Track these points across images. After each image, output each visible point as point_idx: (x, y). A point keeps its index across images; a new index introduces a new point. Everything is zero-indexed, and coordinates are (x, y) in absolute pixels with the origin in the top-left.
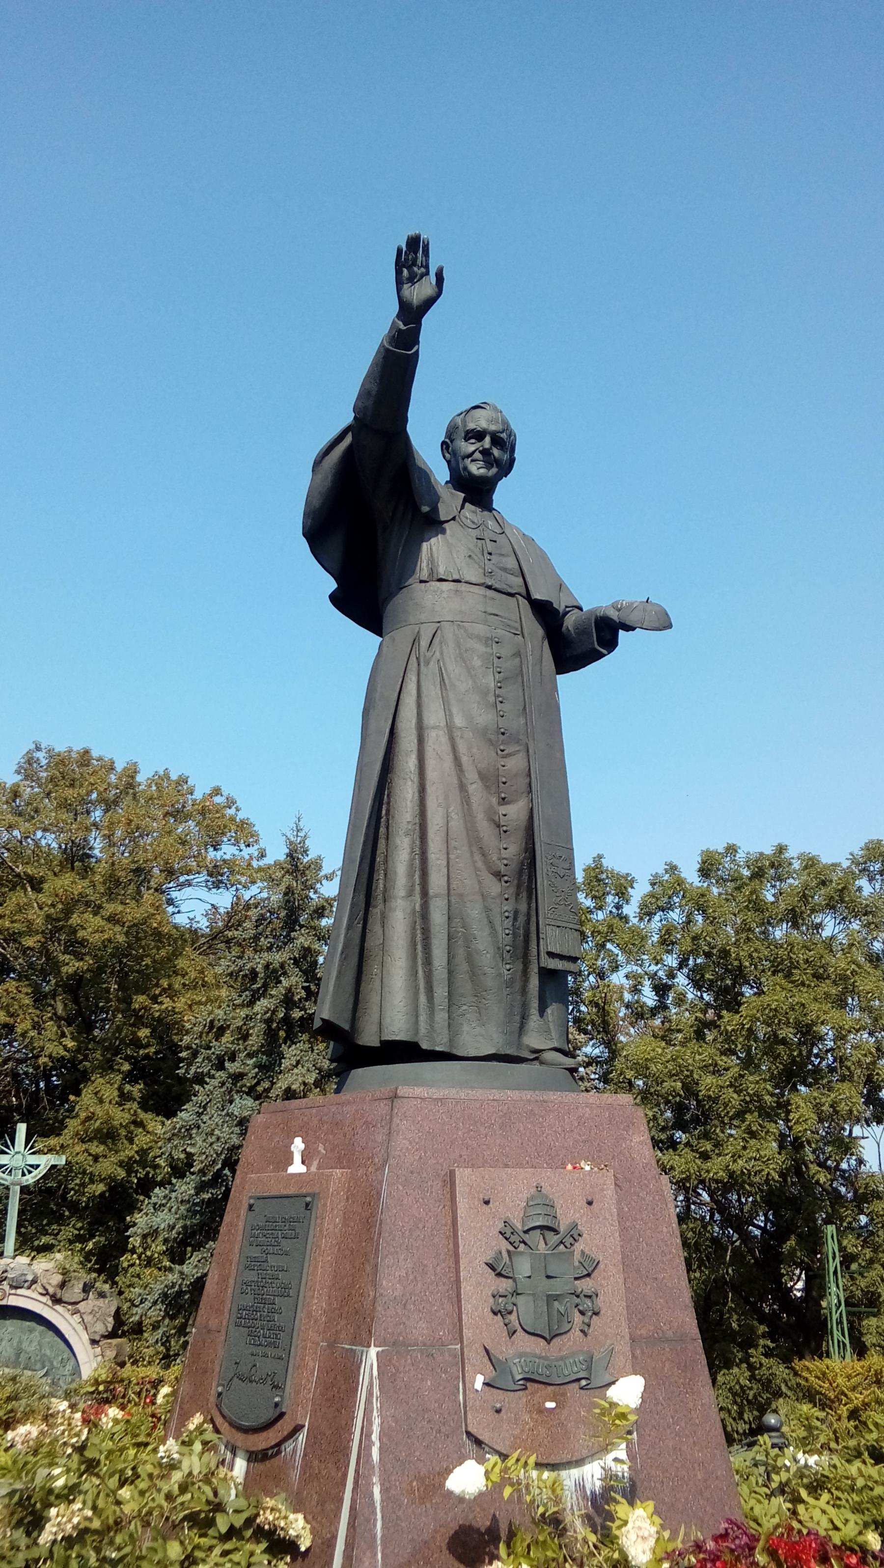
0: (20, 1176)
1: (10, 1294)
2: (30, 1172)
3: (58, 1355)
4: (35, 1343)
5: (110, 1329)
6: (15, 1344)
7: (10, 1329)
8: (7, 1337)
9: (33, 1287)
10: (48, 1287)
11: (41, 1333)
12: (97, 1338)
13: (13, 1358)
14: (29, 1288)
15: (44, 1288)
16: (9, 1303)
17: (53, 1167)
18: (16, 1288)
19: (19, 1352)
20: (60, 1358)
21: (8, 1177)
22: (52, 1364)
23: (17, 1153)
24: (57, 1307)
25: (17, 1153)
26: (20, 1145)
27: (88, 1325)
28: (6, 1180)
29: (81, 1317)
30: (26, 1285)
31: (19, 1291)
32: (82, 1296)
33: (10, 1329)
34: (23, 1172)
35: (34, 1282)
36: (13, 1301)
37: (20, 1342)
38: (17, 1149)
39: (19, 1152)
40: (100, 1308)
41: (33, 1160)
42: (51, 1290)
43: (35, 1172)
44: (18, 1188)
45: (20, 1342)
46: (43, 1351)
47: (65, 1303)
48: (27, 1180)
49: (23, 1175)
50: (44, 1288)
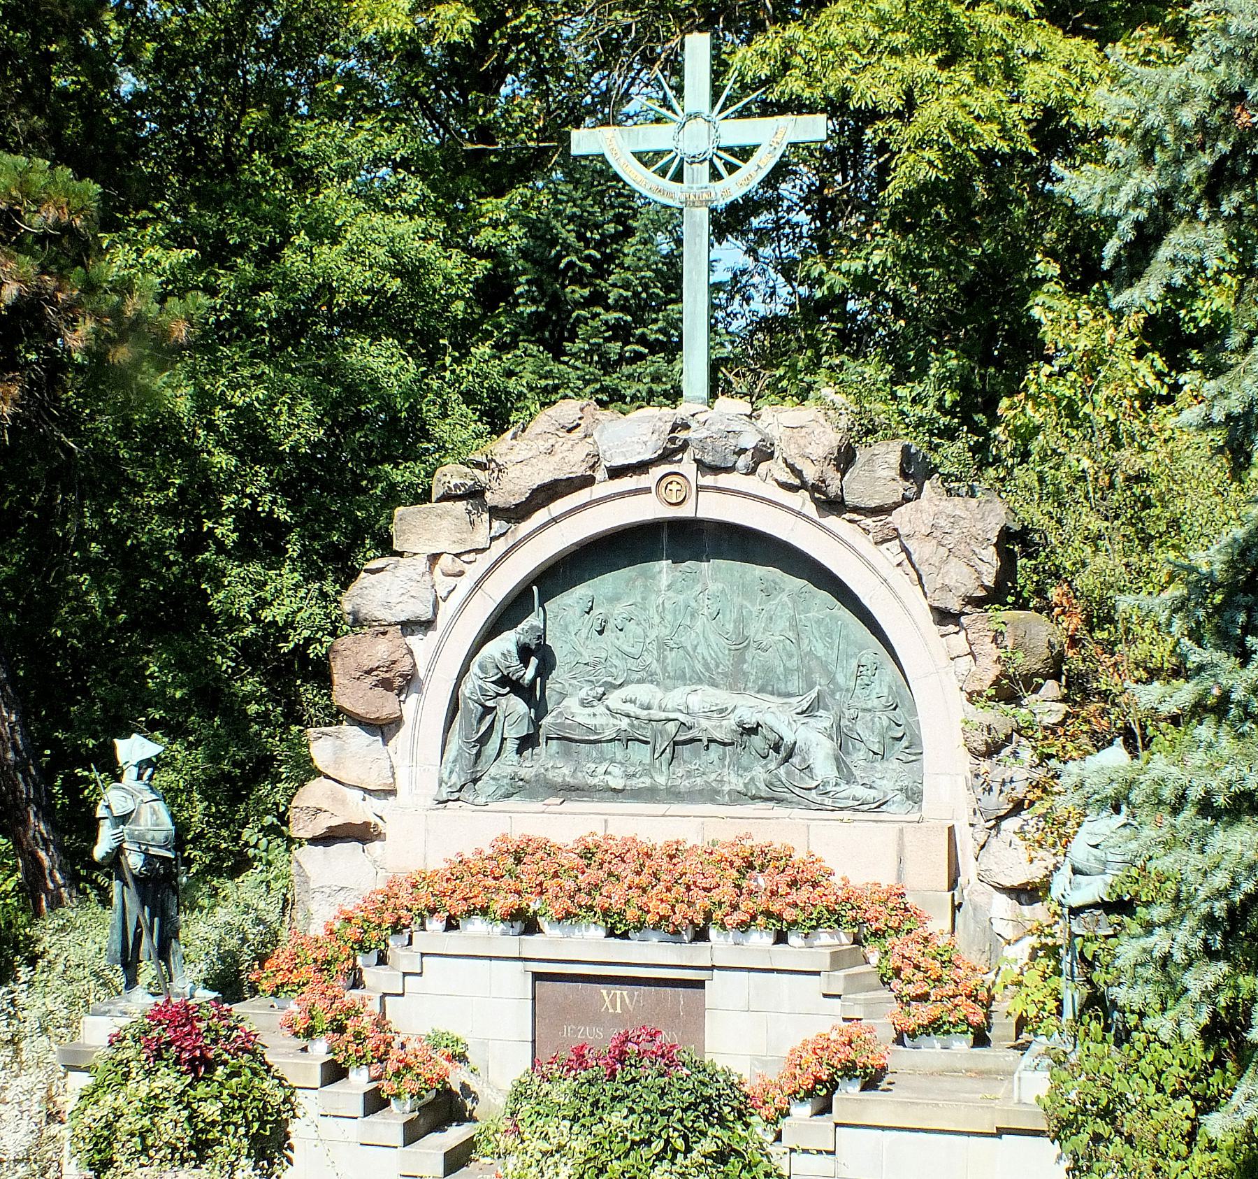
2: (732, 169)
3: (848, 657)
4: (782, 624)
5: (989, 581)
6: (730, 627)
7: (713, 587)
8: (706, 608)
9: (763, 468)
11: (796, 596)
12: (955, 605)
13: (727, 663)
14: (752, 471)
15: (792, 468)
18: (716, 470)
19: (741, 645)
20: (854, 663)
22: (832, 680)
24: (832, 521)
25: (696, 115)
27: (924, 570)
28: (669, 194)
29: (905, 549)
30: (743, 461)
31: (723, 480)
32: (900, 487)
33: (713, 587)
35: (763, 454)
36: (713, 508)
37: (741, 621)
39: (696, 115)
40: (955, 519)
41: (738, 132)
42: (811, 474)
43: (746, 169)
44: (703, 215)
45: (741, 621)
46: (805, 646)
47: (856, 510)
48: (726, 192)
50: (792, 468)
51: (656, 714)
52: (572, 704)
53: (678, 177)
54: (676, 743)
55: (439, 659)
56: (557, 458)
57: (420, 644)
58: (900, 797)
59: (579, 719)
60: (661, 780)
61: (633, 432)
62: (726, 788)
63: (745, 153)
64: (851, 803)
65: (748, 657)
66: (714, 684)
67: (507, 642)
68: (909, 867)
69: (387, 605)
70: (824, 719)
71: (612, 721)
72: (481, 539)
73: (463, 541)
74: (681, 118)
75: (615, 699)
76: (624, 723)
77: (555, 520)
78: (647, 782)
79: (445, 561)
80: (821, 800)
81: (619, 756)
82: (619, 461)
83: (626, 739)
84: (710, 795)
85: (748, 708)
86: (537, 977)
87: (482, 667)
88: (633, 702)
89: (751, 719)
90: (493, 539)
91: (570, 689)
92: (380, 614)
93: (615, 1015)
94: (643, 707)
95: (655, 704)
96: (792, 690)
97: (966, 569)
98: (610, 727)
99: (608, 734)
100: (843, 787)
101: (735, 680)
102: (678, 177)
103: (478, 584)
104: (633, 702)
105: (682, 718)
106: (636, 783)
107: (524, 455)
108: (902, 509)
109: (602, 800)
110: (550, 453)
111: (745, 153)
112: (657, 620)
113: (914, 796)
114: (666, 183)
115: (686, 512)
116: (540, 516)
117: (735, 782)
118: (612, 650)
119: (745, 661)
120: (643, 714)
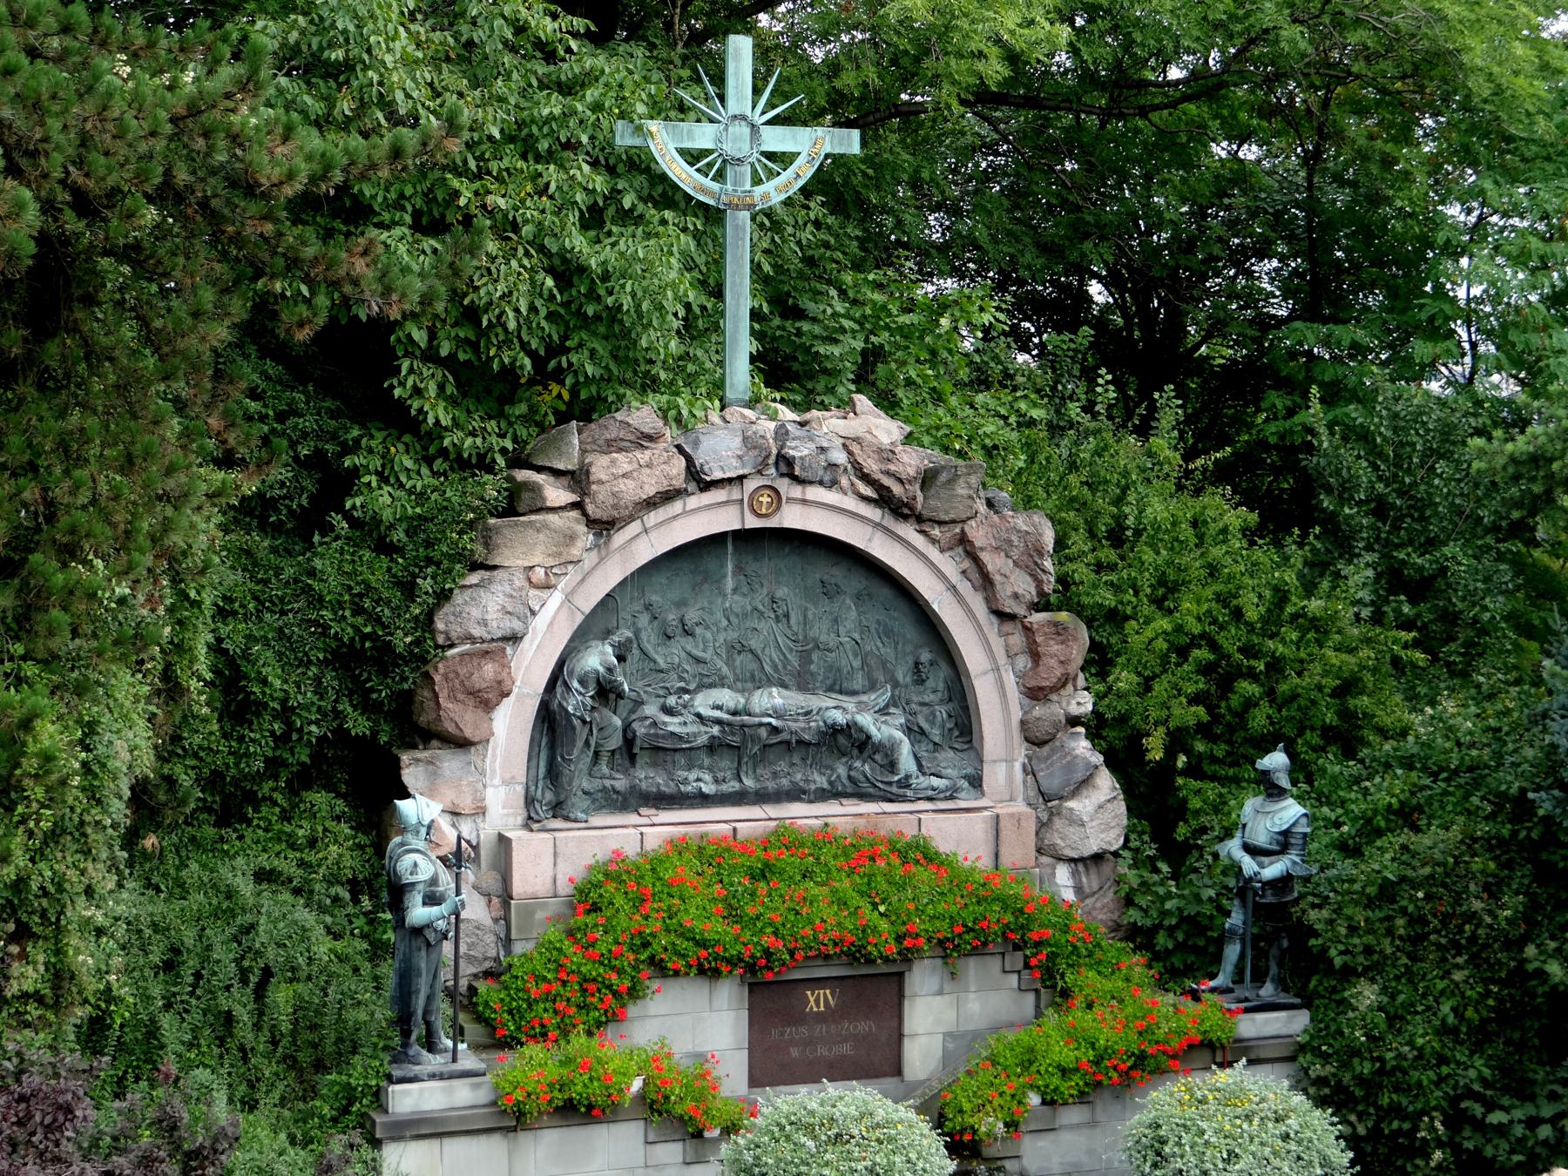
0: (748, 187)
2: (771, 174)
10: (887, 481)
16: (786, 525)
21: (715, 186)
23: (735, 117)
26: (740, 99)
34: (754, 171)
36: (792, 518)
41: (778, 139)
43: (785, 176)
48: (765, 196)
49: (757, 181)
52: (651, 709)
53: (720, 176)
58: (966, 784)
59: (670, 728)
60: (749, 782)
62: (813, 787)
64: (930, 793)
65: (815, 657)
66: (785, 687)
68: (1003, 850)
69: (484, 623)
71: (703, 729)
72: (575, 552)
73: (560, 554)
74: (722, 116)
76: (716, 730)
80: (897, 792)
81: (707, 761)
82: (718, 475)
83: (713, 747)
85: (837, 709)
87: (581, 682)
88: (719, 708)
89: (839, 718)
91: (644, 696)
92: (477, 632)
93: (818, 1013)
94: (728, 712)
96: (857, 685)
97: (1029, 579)
98: (704, 734)
99: (702, 740)
100: (922, 779)
101: (804, 683)
102: (720, 176)
103: (568, 598)
104: (719, 708)
105: (773, 722)
107: (627, 467)
108: (973, 523)
109: (692, 806)
110: (649, 466)
111: (784, 159)
112: (725, 623)
113: (976, 782)
114: (707, 182)
116: (635, 527)
117: (821, 781)
118: (683, 655)
119: (811, 662)
120: (725, 716)
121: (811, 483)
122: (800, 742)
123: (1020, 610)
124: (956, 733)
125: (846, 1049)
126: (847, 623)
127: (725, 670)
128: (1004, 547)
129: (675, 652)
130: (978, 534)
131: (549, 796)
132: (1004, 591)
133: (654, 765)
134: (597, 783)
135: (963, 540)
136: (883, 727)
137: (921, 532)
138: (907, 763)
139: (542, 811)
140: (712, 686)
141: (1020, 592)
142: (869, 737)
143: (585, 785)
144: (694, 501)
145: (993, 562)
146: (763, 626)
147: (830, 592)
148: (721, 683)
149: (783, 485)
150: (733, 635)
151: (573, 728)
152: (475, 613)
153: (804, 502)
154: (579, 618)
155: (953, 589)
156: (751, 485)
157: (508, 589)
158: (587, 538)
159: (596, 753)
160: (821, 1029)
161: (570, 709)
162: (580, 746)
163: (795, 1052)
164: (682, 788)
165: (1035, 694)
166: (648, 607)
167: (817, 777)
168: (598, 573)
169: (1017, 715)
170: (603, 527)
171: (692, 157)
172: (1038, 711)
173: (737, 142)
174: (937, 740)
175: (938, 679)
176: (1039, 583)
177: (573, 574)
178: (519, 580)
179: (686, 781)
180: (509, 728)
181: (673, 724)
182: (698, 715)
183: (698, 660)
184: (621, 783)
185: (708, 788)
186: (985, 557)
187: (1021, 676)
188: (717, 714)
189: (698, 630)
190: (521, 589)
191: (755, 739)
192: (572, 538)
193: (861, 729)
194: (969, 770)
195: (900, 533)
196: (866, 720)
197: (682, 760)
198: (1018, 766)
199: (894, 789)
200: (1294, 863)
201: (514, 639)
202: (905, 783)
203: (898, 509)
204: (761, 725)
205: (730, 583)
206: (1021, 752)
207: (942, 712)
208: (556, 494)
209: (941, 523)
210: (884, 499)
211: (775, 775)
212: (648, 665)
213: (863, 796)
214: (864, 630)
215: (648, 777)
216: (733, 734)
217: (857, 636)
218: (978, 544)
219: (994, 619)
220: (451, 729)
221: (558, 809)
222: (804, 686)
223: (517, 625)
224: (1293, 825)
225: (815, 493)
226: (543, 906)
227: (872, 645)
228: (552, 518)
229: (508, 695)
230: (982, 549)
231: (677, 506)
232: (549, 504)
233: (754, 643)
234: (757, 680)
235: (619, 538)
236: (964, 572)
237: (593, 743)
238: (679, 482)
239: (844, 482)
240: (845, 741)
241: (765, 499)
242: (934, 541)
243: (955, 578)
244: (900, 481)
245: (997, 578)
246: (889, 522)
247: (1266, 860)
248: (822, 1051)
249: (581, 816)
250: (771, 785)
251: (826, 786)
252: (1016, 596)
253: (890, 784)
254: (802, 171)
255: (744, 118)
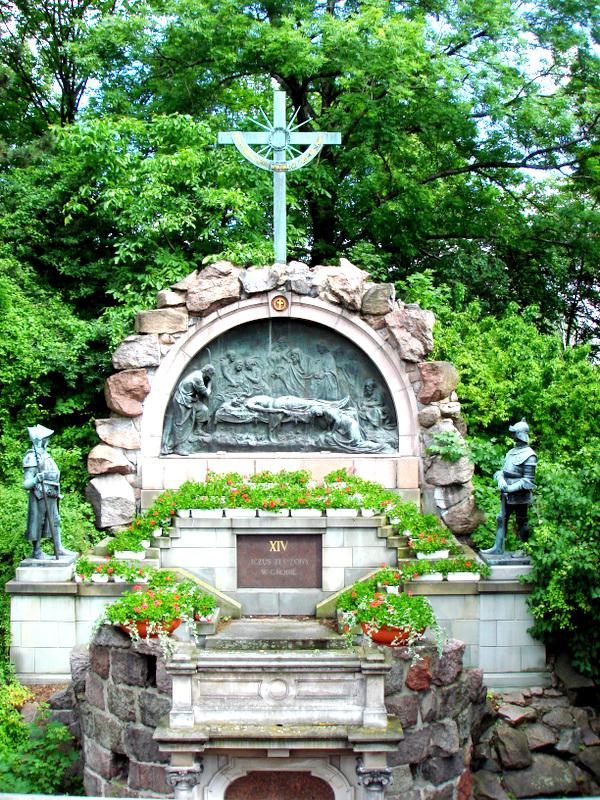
1: (292, 303)
2: (296, 155)
10: (342, 294)
17: (326, 147)
21: (269, 161)
23: (277, 129)
34: (287, 153)
36: (296, 312)
38: (276, 125)
51: (271, 409)
52: (227, 405)
53: (271, 157)
54: (282, 424)
55: (161, 387)
56: (223, 288)
57: (151, 377)
58: (389, 446)
60: (274, 441)
61: (257, 279)
63: (303, 148)
64: (367, 449)
65: (313, 381)
66: (297, 396)
67: (197, 375)
68: (399, 479)
69: (137, 359)
70: (353, 411)
72: (183, 327)
75: (251, 403)
77: (220, 317)
78: (267, 442)
79: (165, 338)
80: (348, 446)
82: (253, 290)
83: (255, 423)
84: (297, 448)
85: (318, 406)
86: (238, 536)
88: (258, 404)
89: (319, 411)
90: (190, 326)
92: (134, 363)
93: (277, 553)
95: (271, 405)
96: (334, 397)
98: (250, 416)
99: (248, 419)
100: (363, 442)
102: (271, 157)
104: (258, 404)
105: (286, 412)
106: (261, 443)
111: (303, 148)
113: (395, 445)
114: (264, 159)
115: (284, 314)
116: (213, 316)
117: (312, 442)
120: (263, 408)
121: (305, 295)
122: (300, 422)
123: (415, 359)
124: (387, 421)
125: (293, 572)
126: (327, 366)
127: (267, 387)
128: (405, 326)
129: (242, 377)
130: (390, 319)
131: (171, 443)
132: (405, 348)
133: (226, 430)
134: (196, 438)
135: (384, 325)
136: (344, 416)
137: (364, 320)
138: (355, 431)
139: (167, 449)
140: (261, 394)
141: (414, 349)
142: (334, 420)
143: (191, 439)
144: (243, 304)
145: (399, 334)
146: (287, 367)
147: (322, 351)
148: (265, 392)
149: (288, 295)
150: (271, 370)
151: (180, 410)
152: (132, 354)
153: (302, 304)
154: (188, 359)
155: (380, 348)
156: (272, 296)
157: (148, 342)
158: (187, 321)
159: (196, 424)
160: (278, 561)
161: (179, 401)
162: (195, 419)
163: (264, 572)
164: (239, 442)
165: (425, 402)
166: (228, 356)
167: (309, 439)
168: (198, 337)
169: (416, 412)
170: (198, 315)
171: (255, 147)
172: (426, 410)
173: (278, 140)
174: (375, 424)
175: (378, 393)
176: (425, 345)
177: (184, 338)
178: (154, 338)
179: (241, 439)
180: (153, 410)
181: (235, 411)
182: (247, 407)
183: (253, 382)
184: (208, 438)
185: (253, 442)
186: (394, 331)
187: (417, 393)
188: (258, 407)
189: (254, 368)
190: (155, 343)
191: (276, 419)
192: (181, 319)
193: (330, 416)
194: (392, 439)
195: (352, 320)
196: (335, 412)
197: (240, 428)
198: (417, 438)
199: (349, 447)
200: (526, 482)
201: (153, 367)
202: (354, 444)
203: (352, 308)
204: (278, 413)
205: (270, 346)
206: (418, 431)
207: (379, 410)
208: (172, 298)
209: (374, 315)
210: (341, 303)
211: (288, 438)
212: (229, 383)
213: (333, 450)
214: (339, 368)
215: (222, 436)
216: (265, 417)
217: (334, 372)
218: (391, 325)
219: (404, 364)
220: (117, 408)
221: (174, 449)
222: (307, 395)
223: (154, 361)
224: (526, 461)
225: (305, 300)
226: (157, 493)
227: (341, 377)
228: (169, 310)
229: (148, 393)
230: (393, 327)
231: (235, 306)
232: (168, 303)
233: (281, 374)
234: (283, 392)
235: (206, 320)
236: (387, 340)
237: (194, 418)
238: (236, 294)
239: (322, 295)
240: (322, 422)
241: (280, 303)
242: (371, 325)
243: (381, 342)
244: (348, 292)
245: (401, 342)
246: (346, 314)
247: (512, 480)
248: (279, 572)
249: (185, 453)
250: (286, 443)
251: (314, 444)
252: (412, 351)
253: (347, 444)
254: (313, 152)
255: (281, 129)
